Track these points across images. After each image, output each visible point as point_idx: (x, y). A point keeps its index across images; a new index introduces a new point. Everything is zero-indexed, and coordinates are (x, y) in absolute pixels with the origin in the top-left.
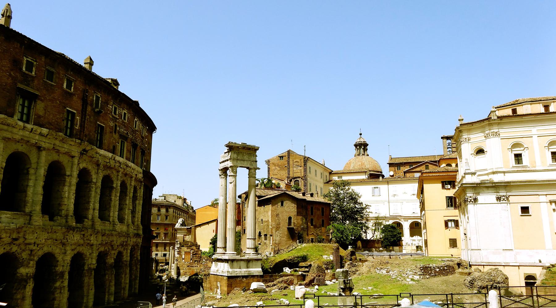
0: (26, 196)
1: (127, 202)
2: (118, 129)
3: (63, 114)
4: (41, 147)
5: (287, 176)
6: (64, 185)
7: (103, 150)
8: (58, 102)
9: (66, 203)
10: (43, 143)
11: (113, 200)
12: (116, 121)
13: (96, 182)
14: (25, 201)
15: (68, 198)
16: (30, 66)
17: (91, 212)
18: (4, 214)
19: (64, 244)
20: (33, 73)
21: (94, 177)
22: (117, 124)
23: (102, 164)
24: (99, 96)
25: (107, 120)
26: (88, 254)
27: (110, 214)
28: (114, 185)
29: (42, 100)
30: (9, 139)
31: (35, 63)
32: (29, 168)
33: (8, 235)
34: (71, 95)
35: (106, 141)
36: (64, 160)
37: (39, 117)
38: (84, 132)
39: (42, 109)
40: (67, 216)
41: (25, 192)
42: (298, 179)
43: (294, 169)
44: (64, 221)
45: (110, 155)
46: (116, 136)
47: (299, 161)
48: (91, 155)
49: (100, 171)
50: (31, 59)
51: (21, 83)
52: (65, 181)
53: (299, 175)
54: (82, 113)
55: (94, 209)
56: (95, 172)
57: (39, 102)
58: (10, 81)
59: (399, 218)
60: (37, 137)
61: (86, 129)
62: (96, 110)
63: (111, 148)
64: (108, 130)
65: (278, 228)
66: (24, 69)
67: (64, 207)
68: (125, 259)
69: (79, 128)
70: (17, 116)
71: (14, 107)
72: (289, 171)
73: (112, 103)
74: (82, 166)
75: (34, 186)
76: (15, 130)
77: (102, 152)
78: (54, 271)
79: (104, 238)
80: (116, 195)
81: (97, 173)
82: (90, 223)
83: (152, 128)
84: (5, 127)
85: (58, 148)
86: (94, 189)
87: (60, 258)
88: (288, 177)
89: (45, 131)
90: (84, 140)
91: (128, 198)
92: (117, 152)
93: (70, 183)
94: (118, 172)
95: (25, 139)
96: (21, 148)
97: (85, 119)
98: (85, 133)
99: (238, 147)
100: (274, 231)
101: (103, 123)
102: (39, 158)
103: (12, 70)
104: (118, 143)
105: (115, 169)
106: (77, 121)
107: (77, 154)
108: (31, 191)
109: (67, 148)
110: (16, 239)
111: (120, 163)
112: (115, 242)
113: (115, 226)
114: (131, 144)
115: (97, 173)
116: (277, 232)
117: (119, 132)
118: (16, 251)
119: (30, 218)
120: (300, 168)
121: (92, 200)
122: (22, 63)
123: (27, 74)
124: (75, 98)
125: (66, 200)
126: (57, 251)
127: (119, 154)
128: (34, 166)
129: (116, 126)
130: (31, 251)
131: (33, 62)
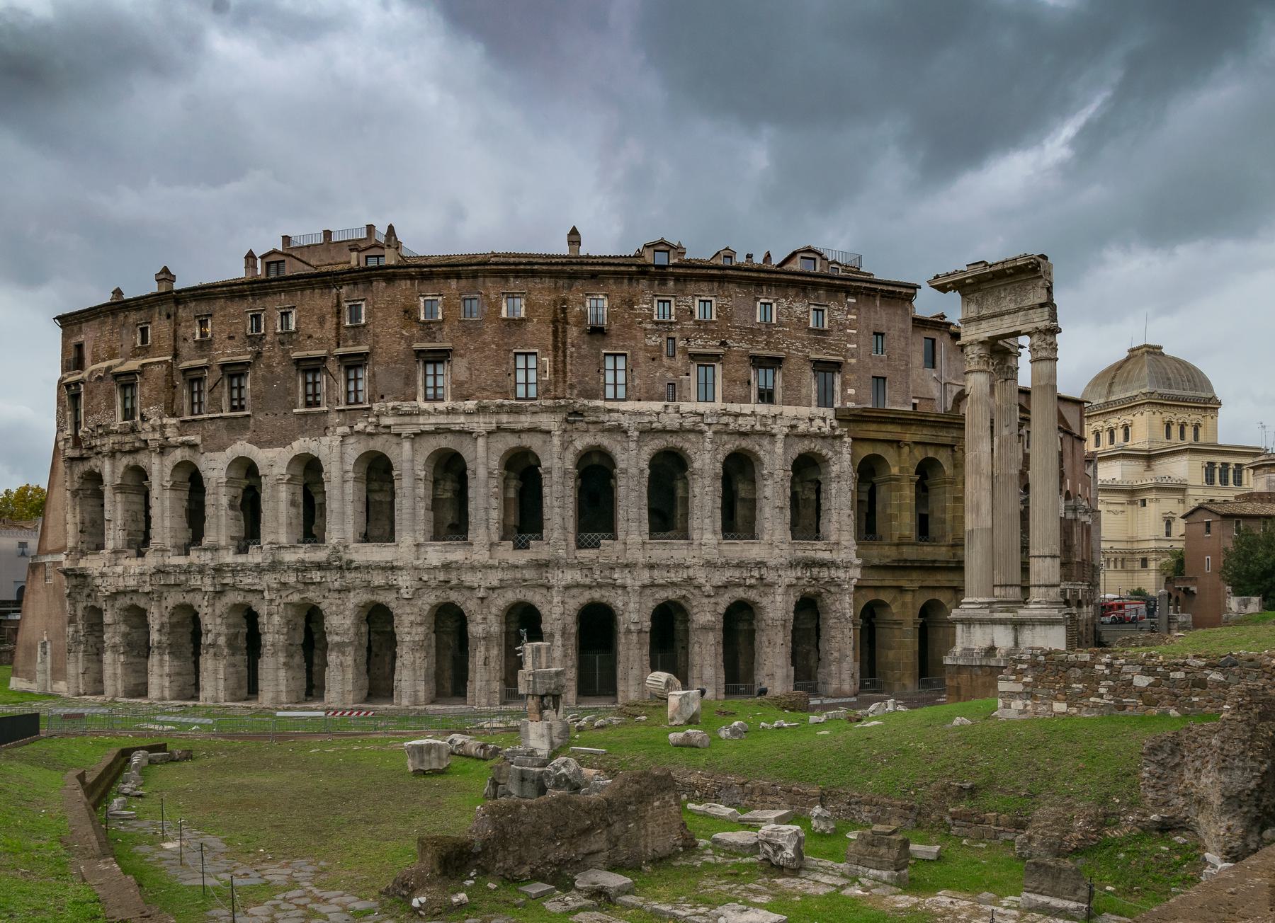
1: (768, 492)
2: (681, 344)
3: (508, 363)
8: (494, 346)
10: (475, 425)
12: (670, 330)
18: (431, 545)
19: (549, 588)
22: (672, 335)
23: (632, 429)
24: (601, 297)
25: (635, 338)
26: (620, 604)
29: (461, 356)
30: (416, 434)
33: (432, 576)
35: (637, 381)
37: (460, 384)
38: (565, 382)
39: (465, 369)
46: (680, 360)
48: (595, 419)
51: (422, 340)
54: (555, 348)
57: (455, 360)
61: (569, 375)
63: (661, 388)
64: (641, 356)
69: (552, 376)
70: (420, 398)
71: (415, 384)
73: (648, 297)
74: (581, 443)
76: (421, 420)
79: (656, 573)
84: (407, 419)
89: (471, 405)
90: (568, 396)
91: (769, 482)
92: (685, 393)
94: (702, 432)
95: (441, 426)
96: (445, 442)
97: (565, 356)
98: (568, 383)
101: (623, 347)
104: (688, 374)
106: (544, 366)
109: (529, 420)
111: (703, 415)
114: (747, 364)
117: (684, 350)
124: (530, 327)
127: (694, 396)
130: (482, 599)
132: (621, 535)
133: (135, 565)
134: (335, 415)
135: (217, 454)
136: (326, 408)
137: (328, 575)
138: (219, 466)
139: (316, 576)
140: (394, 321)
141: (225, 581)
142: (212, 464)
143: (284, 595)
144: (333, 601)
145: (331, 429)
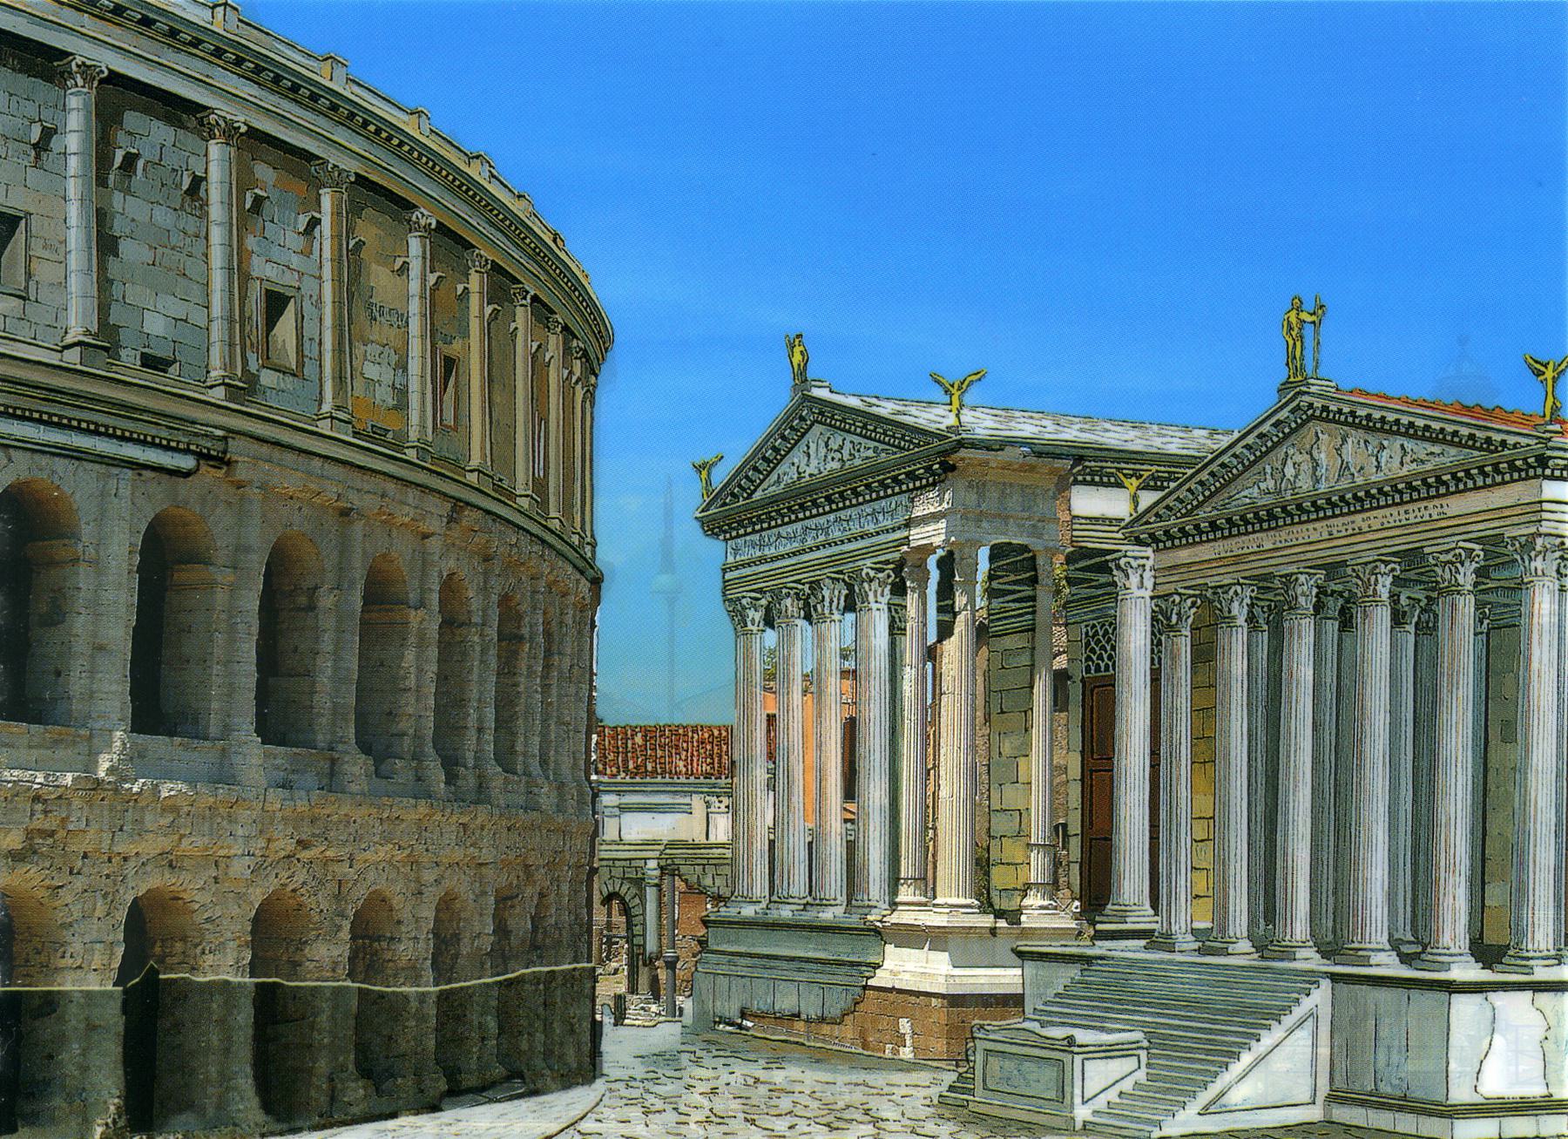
21: (475, 605)
27: (513, 746)
28: (525, 631)
32: (316, 588)
36: (402, 549)
44: (411, 775)
55: (480, 730)
56: (478, 585)
68: (553, 921)
78: (388, 956)
80: (530, 667)
108: (329, 672)
113: (536, 790)
115: (485, 590)
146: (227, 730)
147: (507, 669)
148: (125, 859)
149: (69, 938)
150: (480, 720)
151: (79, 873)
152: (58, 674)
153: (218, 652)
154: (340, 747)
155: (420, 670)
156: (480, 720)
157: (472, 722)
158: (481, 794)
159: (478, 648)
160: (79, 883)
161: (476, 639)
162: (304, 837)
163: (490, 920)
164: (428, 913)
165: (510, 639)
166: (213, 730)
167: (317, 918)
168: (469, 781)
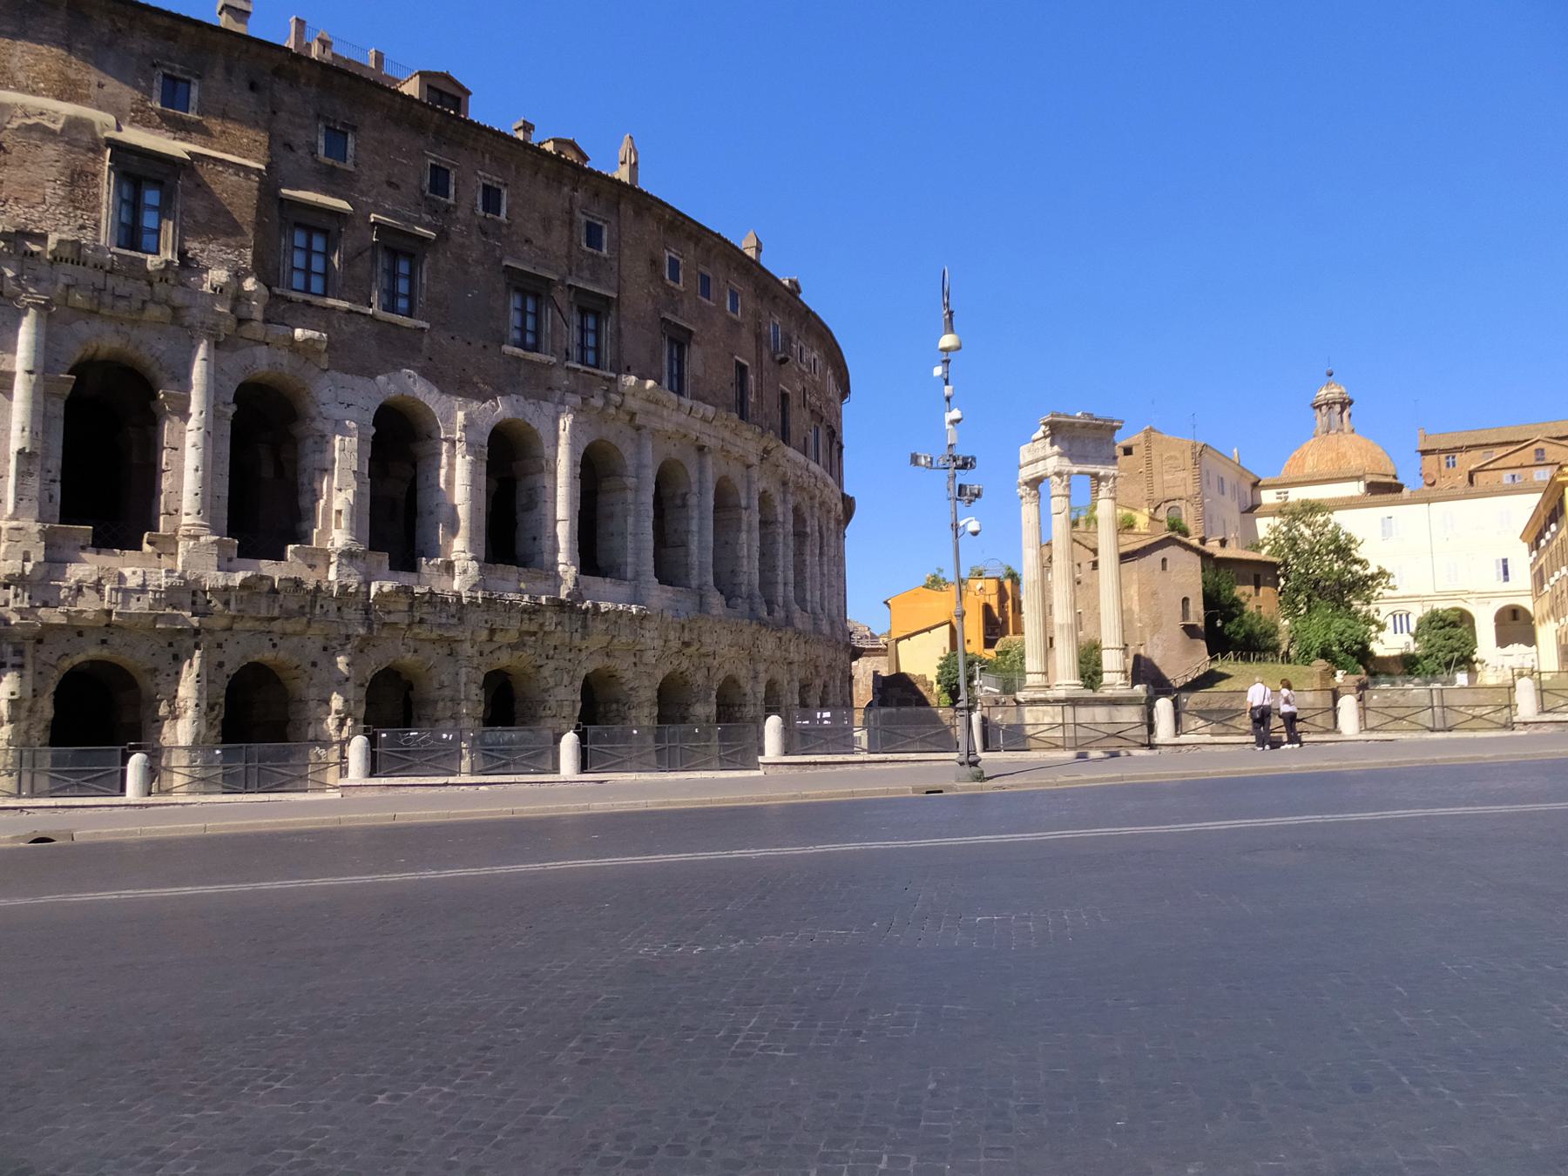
0: (687, 555)
4: (705, 446)
5: (1146, 497)
6: (739, 530)
7: (791, 449)
9: (745, 569)
11: (808, 563)
13: (784, 522)
14: (687, 564)
15: (749, 556)
16: (674, 264)
17: (781, 588)
20: (681, 284)
21: (780, 509)
22: (806, 386)
28: (808, 530)
29: (698, 344)
31: (681, 262)
32: (686, 494)
33: (677, 635)
34: (736, 325)
36: (735, 472)
40: (750, 596)
41: (684, 545)
42: (1177, 503)
43: (1165, 478)
44: (747, 607)
45: (801, 458)
47: (1178, 455)
49: (789, 497)
50: (676, 254)
52: (739, 519)
53: (1179, 492)
55: (785, 584)
58: (650, 307)
59: (1464, 597)
60: (698, 425)
62: (778, 357)
65: (1156, 626)
66: (667, 277)
67: (744, 579)
72: (1150, 484)
75: (700, 531)
77: (791, 452)
78: (738, 715)
80: (812, 551)
81: (785, 501)
82: (782, 614)
83: (845, 390)
85: (729, 447)
86: (781, 538)
87: (748, 689)
88: (1150, 500)
93: (750, 525)
99: (1072, 425)
100: (1148, 637)
102: (702, 470)
103: (651, 282)
105: (808, 492)
107: (754, 460)
108: (696, 543)
110: (686, 644)
112: (822, 658)
113: (819, 622)
115: (785, 501)
116: (1155, 637)
117: (810, 404)
118: (688, 668)
119: (701, 601)
120: (1182, 475)
121: (781, 563)
122: (662, 265)
123: (673, 288)
125: (745, 562)
126: (743, 674)
128: (695, 489)
129: (804, 389)
131: (678, 258)
132: (780, 600)
133: (132, 568)
134: (563, 373)
135: (359, 382)
136: (554, 360)
137: (567, 621)
138: (361, 402)
139: (550, 619)
140: (642, 268)
141: (392, 618)
142: (347, 396)
143: (486, 651)
144: (563, 664)
145: (558, 394)
146: (637, 575)
147: (799, 553)
148: (580, 650)
149: (547, 698)
150: (785, 577)
151: (552, 658)
152: (535, 539)
153: (630, 528)
154: (705, 588)
155: (749, 546)
156: (785, 577)
157: (780, 579)
158: (789, 621)
159: (782, 536)
160: (552, 664)
161: (781, 530)
162: (686, 640)
163: (797, 696)
164: (762, 689)
165: (800, 535)
166: (629, 575)
167: (695, 690)
168: (780, 614)
